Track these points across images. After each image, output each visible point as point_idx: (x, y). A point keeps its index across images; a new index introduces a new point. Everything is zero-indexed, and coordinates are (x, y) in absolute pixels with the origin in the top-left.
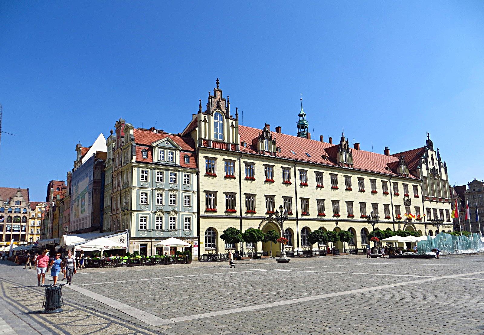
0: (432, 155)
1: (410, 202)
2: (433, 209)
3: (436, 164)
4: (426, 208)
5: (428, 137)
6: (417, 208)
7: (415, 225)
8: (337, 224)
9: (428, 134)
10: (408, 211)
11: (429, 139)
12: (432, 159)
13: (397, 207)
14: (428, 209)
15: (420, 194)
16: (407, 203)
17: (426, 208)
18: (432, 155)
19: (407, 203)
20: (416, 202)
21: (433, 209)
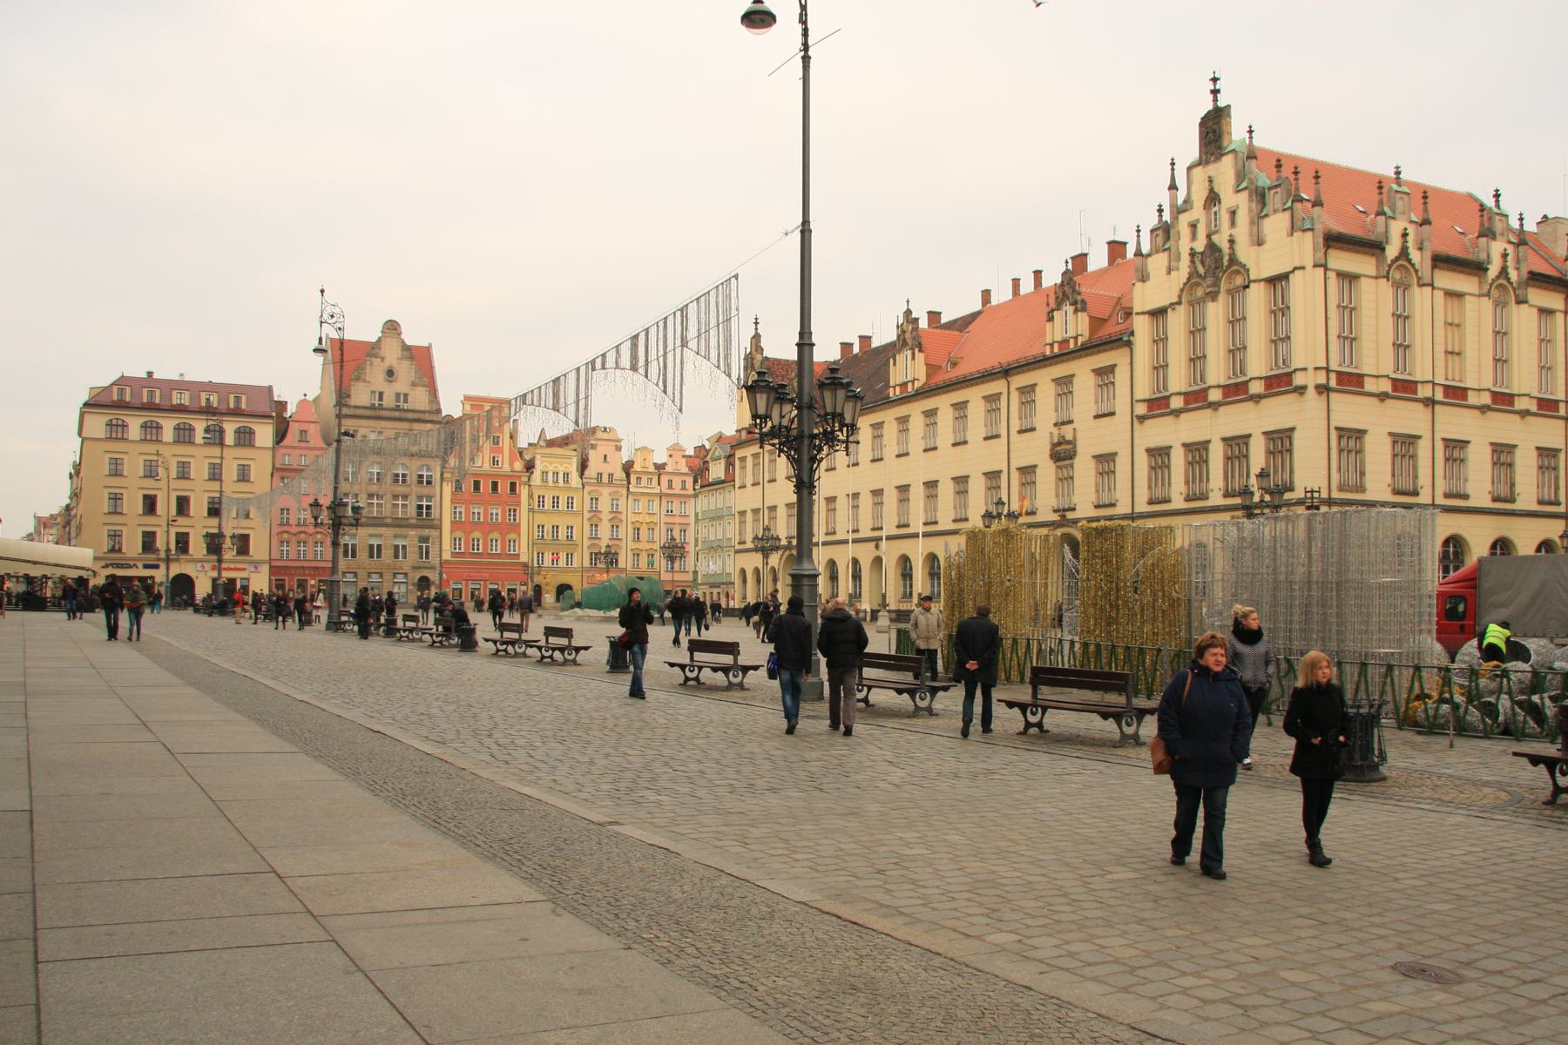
0: (1211, 181)
1: (1073, 443)
2: (1185, 445)
3: (1233, 213)
4: (1149, 451)
5: (1215, 92)
6: (1105, 461)
8: (877, 547)
10: (1066, 480)
11: (1215, 100)
12: (1213, 199)
13: (1028, 471)
16: (1063, 453)
17: (1149, 451)
18: (1211, 181)
19: (1063, 453)
20: (1091, 439)
21: (1185, 445)
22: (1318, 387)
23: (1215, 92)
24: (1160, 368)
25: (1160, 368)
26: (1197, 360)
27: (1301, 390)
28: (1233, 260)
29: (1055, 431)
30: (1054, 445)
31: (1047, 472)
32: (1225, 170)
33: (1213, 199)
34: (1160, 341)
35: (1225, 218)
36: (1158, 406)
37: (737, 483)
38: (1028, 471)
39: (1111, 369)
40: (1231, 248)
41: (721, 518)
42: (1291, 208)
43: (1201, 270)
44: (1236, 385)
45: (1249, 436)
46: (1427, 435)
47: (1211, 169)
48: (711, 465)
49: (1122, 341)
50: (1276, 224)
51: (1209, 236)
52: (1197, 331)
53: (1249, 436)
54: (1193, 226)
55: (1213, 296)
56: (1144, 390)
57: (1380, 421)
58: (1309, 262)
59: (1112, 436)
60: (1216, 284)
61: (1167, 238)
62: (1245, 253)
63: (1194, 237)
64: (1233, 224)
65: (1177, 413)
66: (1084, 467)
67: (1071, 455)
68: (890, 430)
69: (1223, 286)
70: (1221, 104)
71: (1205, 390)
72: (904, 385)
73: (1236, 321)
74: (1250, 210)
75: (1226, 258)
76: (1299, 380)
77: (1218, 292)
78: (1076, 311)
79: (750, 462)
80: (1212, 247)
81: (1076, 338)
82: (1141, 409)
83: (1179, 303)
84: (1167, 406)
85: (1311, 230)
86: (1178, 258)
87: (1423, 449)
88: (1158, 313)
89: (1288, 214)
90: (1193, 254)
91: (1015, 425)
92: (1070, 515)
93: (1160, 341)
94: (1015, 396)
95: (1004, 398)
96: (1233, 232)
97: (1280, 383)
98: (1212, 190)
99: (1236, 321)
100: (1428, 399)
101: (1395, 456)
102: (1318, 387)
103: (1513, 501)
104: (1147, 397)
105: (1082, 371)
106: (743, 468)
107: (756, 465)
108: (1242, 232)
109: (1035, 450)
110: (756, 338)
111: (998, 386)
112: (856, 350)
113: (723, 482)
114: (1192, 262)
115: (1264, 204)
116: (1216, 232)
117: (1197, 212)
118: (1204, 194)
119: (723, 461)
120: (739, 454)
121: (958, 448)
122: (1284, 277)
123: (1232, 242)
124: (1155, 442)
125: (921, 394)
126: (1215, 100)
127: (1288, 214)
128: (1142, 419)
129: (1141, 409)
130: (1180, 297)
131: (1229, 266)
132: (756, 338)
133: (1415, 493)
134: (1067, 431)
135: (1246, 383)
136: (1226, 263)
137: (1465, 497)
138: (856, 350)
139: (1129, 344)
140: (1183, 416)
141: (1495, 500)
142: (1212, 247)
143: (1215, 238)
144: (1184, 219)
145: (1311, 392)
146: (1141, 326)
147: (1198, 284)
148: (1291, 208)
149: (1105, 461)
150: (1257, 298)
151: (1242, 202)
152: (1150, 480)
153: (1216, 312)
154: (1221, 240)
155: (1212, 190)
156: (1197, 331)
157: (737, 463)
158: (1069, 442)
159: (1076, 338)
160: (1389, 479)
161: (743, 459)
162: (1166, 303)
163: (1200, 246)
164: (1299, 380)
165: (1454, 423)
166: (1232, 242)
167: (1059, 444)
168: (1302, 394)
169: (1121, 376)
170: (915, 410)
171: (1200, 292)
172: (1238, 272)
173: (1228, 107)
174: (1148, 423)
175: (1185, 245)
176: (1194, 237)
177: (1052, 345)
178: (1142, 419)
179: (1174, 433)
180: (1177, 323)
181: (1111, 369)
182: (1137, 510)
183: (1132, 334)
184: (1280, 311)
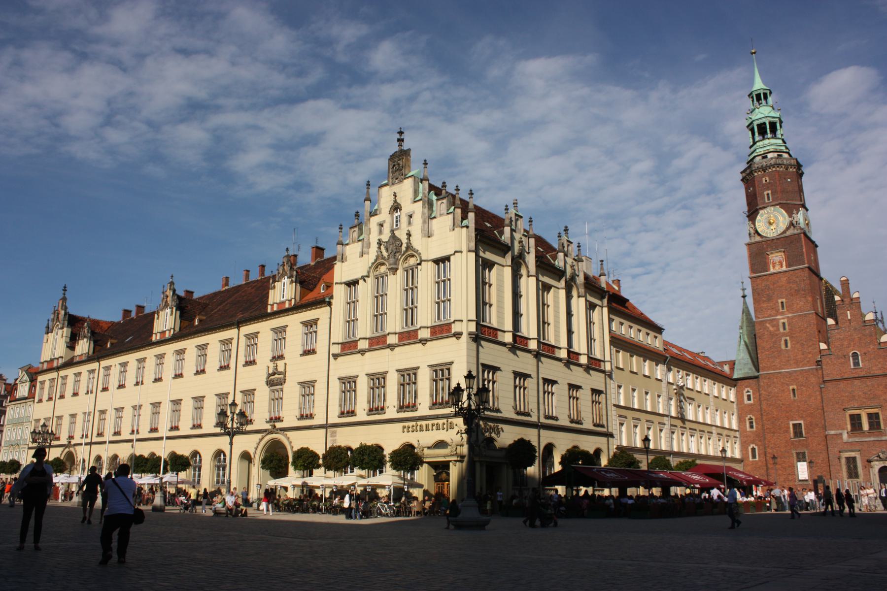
0: (395, 195)
1: (284, 373)
3: (411, 216)
5: (401, 140)
6: (308, 386)
7: (289, 434)
9: (401, 133)
10: (277, 400)
12: (396, 207)
14: (349, 383)
15: (321, 346)
16: (275, 381)
18: (395, 195)
19: (275, 381)
20: (298, 369)
21: (368, 375)
22: (470, 334)
23: (401, 140)
24: (351, 322)
25: (351, 322)
26: (379, 316)
27: (458, 335)
28: (409, 247)
29: (271, 365)
30: (269, 375)
31: (263, 394)
32: (405, 189)
33: (396, 207)
34: (352, 303)
35: (404, 220)
36: (349, 347)
37: (36, 399)
38: (249, 393)
39: (315, 322)
40: (409, 239)
41: (22, 423)
42: (453, 213)
43: (385, 254)
44: (408, 332)
45: (418, 368)
46: (534, 375)
47: (396, 188)
48: (19, 386)
49: (325, 301)
50: (443, 222)
51: (392, 231)
52: (380, 297)
53: (418, 368)
54: (381, 225)
55: (394, 270)
56: (339, 335)
57: (509, 363)
58: (464, 249)
59: (313, 368)
60: (396, 262)
61: (361, 234)
62: (418, 242)
63: (381, 232)
64: (409, 223)
65: (363, 352)
66: (291, 392)
67: (282, 382)
68: (151, 363)
69: (401, 266)
70: (405, 147)
71: (385, 336)
72: (163, 333)
73: (410, 289)
74: (423, 213)
75: (404, 245)
76: (455, 328)
77: (397, 269)
78: (292, 282)
79: (47, 385)
80: (394, 237)
81: (290, 301)
82: (336, 349)
83: (368, 276)
84: (356, 347)
85: (467, 227)
86: (369, 246)
87: (530, 383)
88: (352, 284)
89: (451, 216)
90: (380, 243)
91: (242, 360)
92: (279, 425)
93: (352, 303)
94: (243, 340)
95: (235, 342)
96: (410, 228)
97: (441, 331)
98: (395, 201)
99: (410, 289)
100: (534, 351)
101: (515, 387)
102: (470, 334)
103: (582, 424)
104: (341, 341)
105: (294, 322)
106: (42, 389)
107: (51, 387)
108: (417, 228)
109: (255, 378)
110: (64, 299)
111: (231, 333)
112: (133, 315)
113: (26, 398)
114: (379, 248)
115: (432, 211)
116: (397, 229)
117: (384, 215)
118: (391, 203)
119: (28, 384)
120: (40, 378)
121: (199, 376)
122: (447, 259)
123: (409, 235)
124: (345, 373)
125: (175, 338)
126: (400, 145)
127: (451, 216)
128: (336, 356)
129: (336, 349)
130: (368, 272)
131: (405, 252)
132: (64, 299)
133: (528, 415)
134: (280, 364)
135: (416, 331)
136: (403, 248)
137: (556, 419)
138: (133, 315)
139: (330, 304)
140: (367, 354)
141: (572, 421)
142: (394, 237)
143: (397, 233)
144: (374, 221)
145: (465, 337)
146: (339, 293)
147: (383, 264)
148: (453, 213)
149: (308, 386)
150: (426, 275)
151: (418, 209)
152: (340, 400)
153: (395, 283)
154: (402, 235)
155: (395, 201)
156: (380, 297)
157: (38, 385)
158: (280, 373)
159: (290, 301)
160: (512, 403)
161: (43, 383)
162: (358, 276)
163: (386, 237)
164: (455, 328)
165: (549, 368)
166: (409, 235)
167: (274, 374)
168: (458, 338)
169: (322, 328)
170: (169, 349)
171: (383, 269)
172: (413, 256)
173: (409, 150)
174: (340, 359)
175: (374, 238)
176: (381, 232)
177: (272, 305)
178: (336, 356)
179: (359, 366)
180: (365, 290)
181: (315, 322)
182: (330, 422)
183: (332, 297)
184: (442, 284)
